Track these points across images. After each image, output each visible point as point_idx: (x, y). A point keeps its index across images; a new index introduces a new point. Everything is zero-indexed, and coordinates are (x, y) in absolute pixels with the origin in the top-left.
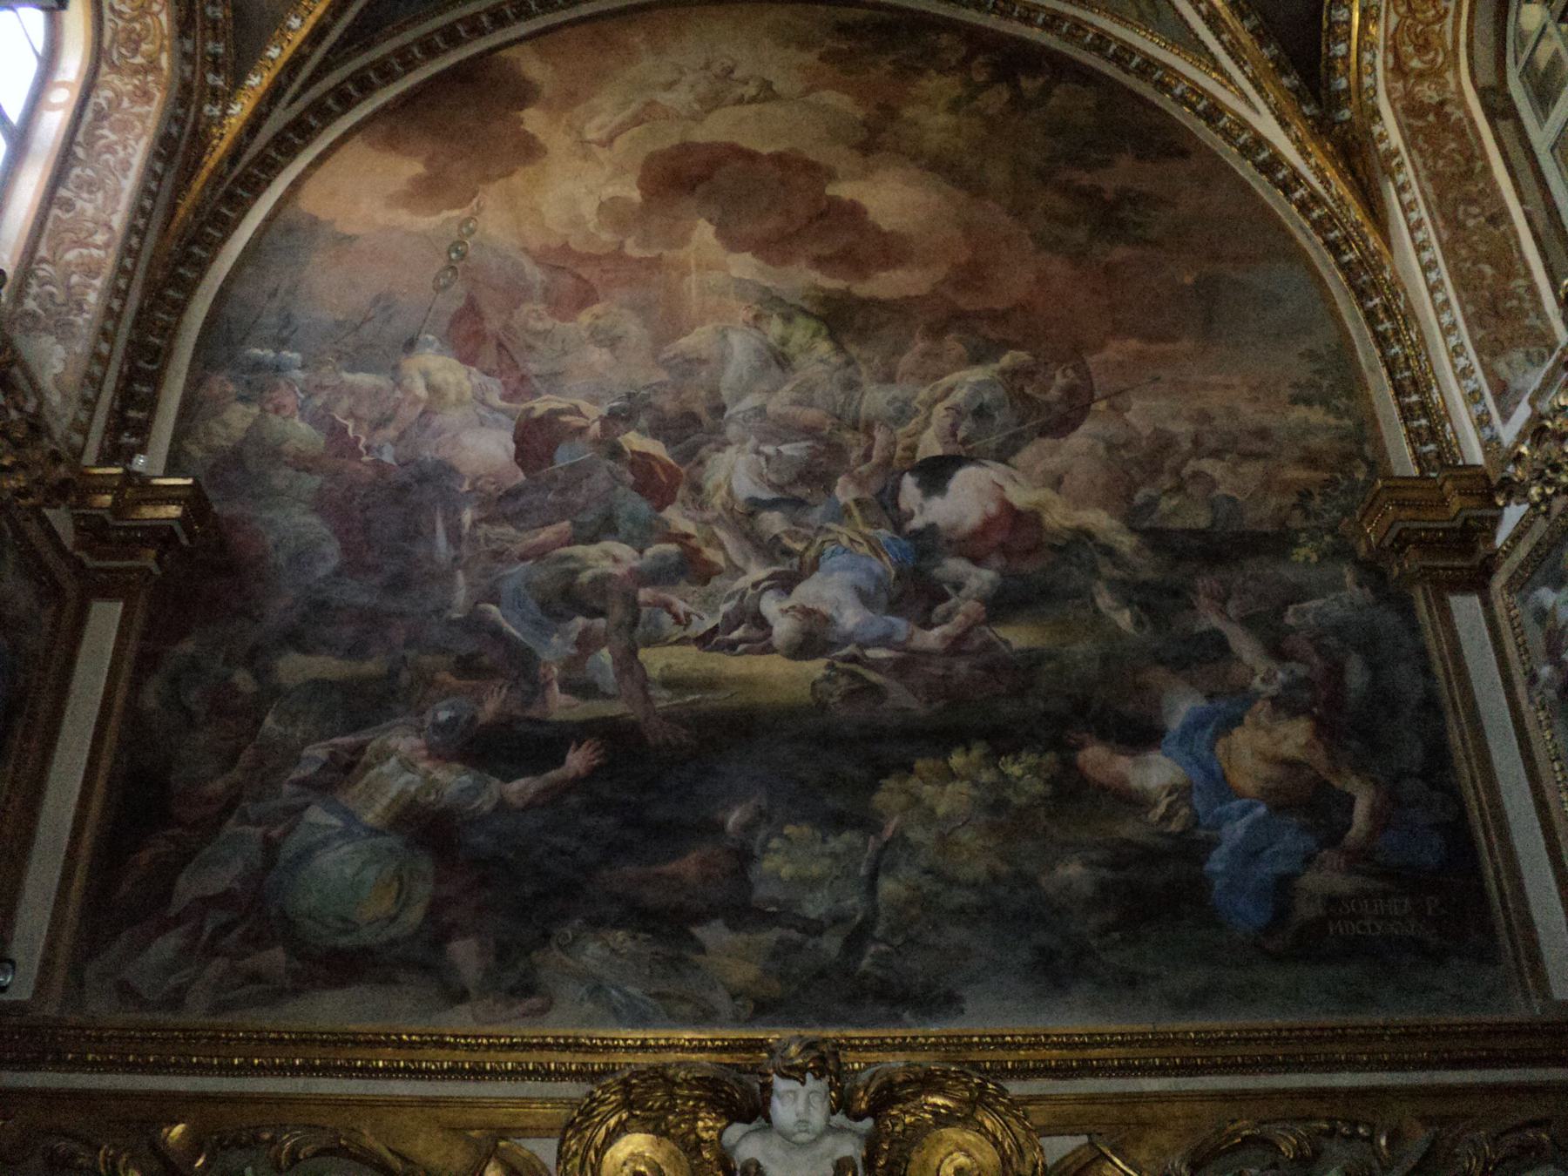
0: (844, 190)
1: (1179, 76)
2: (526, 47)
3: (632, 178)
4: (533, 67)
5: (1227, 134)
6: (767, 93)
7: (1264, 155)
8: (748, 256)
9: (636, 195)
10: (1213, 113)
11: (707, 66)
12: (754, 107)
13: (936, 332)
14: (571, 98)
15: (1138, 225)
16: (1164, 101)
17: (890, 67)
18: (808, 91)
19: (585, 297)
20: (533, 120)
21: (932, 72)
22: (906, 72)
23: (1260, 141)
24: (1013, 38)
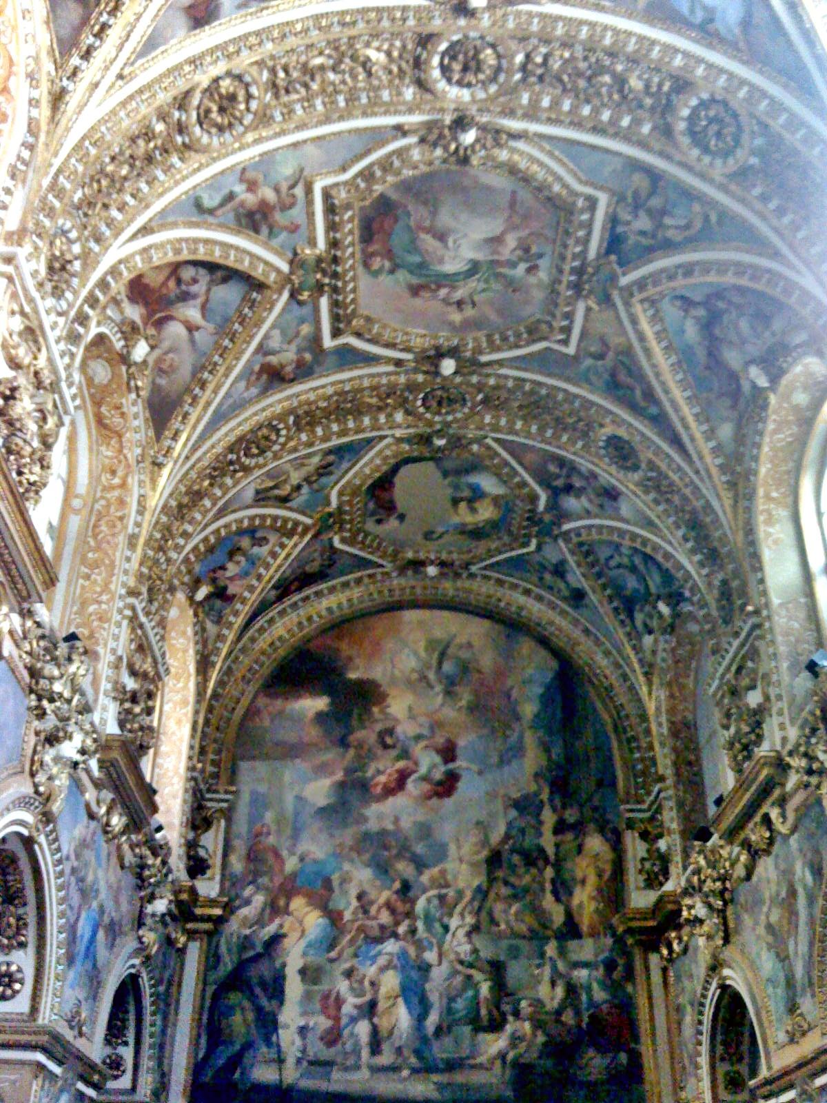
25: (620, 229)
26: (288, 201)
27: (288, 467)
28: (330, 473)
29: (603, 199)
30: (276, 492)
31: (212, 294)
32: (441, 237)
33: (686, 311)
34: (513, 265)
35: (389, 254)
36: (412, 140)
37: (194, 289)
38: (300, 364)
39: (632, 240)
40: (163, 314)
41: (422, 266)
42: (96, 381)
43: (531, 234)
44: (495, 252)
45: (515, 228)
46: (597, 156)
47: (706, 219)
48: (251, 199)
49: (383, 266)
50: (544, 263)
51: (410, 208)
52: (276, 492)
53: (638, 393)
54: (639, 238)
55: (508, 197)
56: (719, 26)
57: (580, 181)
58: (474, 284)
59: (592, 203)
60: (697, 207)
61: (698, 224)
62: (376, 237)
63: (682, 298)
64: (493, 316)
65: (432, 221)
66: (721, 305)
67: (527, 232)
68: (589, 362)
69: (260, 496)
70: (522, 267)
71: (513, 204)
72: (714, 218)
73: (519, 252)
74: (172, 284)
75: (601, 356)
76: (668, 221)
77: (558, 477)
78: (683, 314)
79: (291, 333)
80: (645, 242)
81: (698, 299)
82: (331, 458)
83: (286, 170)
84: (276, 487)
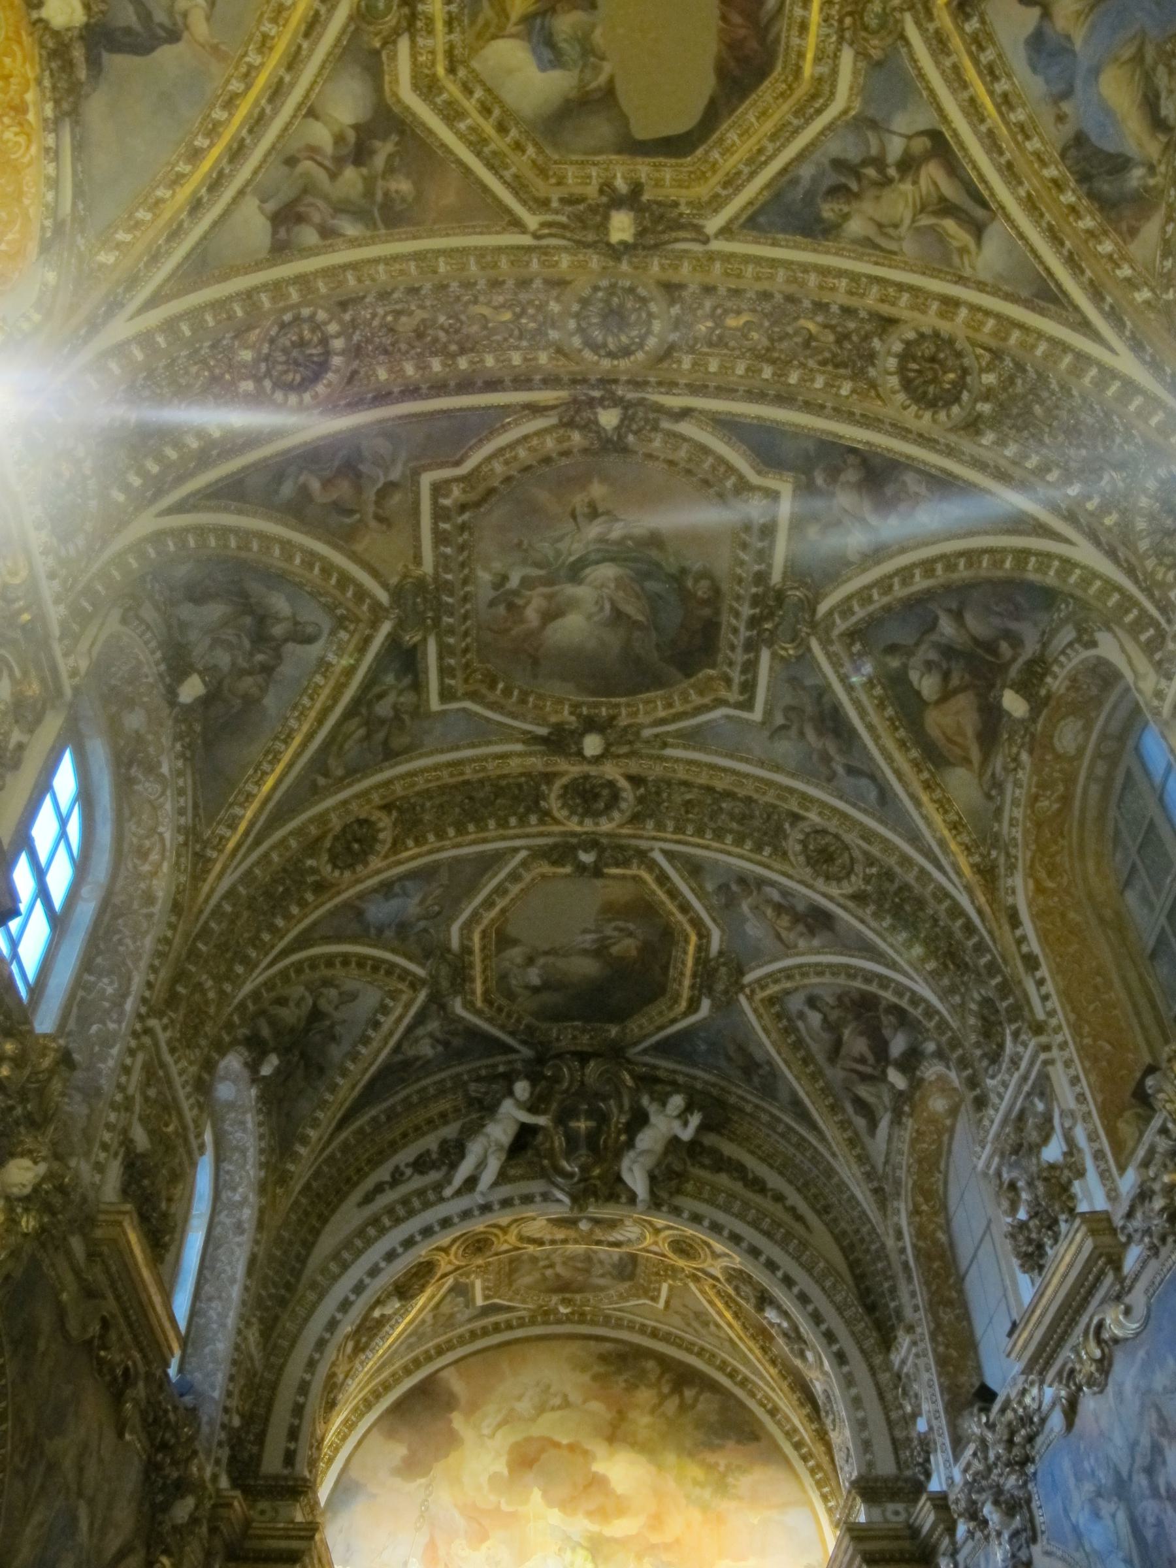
0: (599, 1467)
1: (760, 1388)
2: (452, 1369)
3: (503, 1460)
4: (456, 1383)
5: (779, 1423)
6: (566, 1404)
7: (796, 1439)
8: (556, 1510)
9: (505, 1472)
10: (773, 1412)
11: (538, 1384)
12: (558, 1414)
13: (639, 1557)
14: (473, 1407)
15: (735, 1486)
16: (751, 1404)
17: (623, 1385)
18: (585, 1402)
19: (483, 1537)
20: (457, 1420)
21: (643, 1388)
22: (632, 1387)
23: (795, 1430)
24: (680, 1363)
25: (407, 681)
27: (909, 247)
28: (839, 164)
30: (949, 189)
32: (618, 616)
33: (296, 623)
34: (526, 583)
35: (685, 596)
36: (647, 733)
38: (834, 474)
39: (390, 679)
40: (980, 651)
42: (1080, 724)
43: (508, 630)
44: (550, 597)
47: (326, 775)
48: (832, 750)
52: (949, 189)
53: (315, 485)
57: (464, 710)
58: (575, 546)
60: (340, 772)
61: (332, 762)
63: (310, 640)
64: (542, 496)
66: (260, 657)
67: (513, 633)
68: (395, 475)
69: (979, 213)
70: (514, 582)
72: (321, 781)
73: (520, 602)
74: (955, 681)
76: (362, 732)
77: (390, 170)
80: (377, 690)
81: (290, 646)
82: (828, 210)
83: (784, 747)
84: (946, 208)
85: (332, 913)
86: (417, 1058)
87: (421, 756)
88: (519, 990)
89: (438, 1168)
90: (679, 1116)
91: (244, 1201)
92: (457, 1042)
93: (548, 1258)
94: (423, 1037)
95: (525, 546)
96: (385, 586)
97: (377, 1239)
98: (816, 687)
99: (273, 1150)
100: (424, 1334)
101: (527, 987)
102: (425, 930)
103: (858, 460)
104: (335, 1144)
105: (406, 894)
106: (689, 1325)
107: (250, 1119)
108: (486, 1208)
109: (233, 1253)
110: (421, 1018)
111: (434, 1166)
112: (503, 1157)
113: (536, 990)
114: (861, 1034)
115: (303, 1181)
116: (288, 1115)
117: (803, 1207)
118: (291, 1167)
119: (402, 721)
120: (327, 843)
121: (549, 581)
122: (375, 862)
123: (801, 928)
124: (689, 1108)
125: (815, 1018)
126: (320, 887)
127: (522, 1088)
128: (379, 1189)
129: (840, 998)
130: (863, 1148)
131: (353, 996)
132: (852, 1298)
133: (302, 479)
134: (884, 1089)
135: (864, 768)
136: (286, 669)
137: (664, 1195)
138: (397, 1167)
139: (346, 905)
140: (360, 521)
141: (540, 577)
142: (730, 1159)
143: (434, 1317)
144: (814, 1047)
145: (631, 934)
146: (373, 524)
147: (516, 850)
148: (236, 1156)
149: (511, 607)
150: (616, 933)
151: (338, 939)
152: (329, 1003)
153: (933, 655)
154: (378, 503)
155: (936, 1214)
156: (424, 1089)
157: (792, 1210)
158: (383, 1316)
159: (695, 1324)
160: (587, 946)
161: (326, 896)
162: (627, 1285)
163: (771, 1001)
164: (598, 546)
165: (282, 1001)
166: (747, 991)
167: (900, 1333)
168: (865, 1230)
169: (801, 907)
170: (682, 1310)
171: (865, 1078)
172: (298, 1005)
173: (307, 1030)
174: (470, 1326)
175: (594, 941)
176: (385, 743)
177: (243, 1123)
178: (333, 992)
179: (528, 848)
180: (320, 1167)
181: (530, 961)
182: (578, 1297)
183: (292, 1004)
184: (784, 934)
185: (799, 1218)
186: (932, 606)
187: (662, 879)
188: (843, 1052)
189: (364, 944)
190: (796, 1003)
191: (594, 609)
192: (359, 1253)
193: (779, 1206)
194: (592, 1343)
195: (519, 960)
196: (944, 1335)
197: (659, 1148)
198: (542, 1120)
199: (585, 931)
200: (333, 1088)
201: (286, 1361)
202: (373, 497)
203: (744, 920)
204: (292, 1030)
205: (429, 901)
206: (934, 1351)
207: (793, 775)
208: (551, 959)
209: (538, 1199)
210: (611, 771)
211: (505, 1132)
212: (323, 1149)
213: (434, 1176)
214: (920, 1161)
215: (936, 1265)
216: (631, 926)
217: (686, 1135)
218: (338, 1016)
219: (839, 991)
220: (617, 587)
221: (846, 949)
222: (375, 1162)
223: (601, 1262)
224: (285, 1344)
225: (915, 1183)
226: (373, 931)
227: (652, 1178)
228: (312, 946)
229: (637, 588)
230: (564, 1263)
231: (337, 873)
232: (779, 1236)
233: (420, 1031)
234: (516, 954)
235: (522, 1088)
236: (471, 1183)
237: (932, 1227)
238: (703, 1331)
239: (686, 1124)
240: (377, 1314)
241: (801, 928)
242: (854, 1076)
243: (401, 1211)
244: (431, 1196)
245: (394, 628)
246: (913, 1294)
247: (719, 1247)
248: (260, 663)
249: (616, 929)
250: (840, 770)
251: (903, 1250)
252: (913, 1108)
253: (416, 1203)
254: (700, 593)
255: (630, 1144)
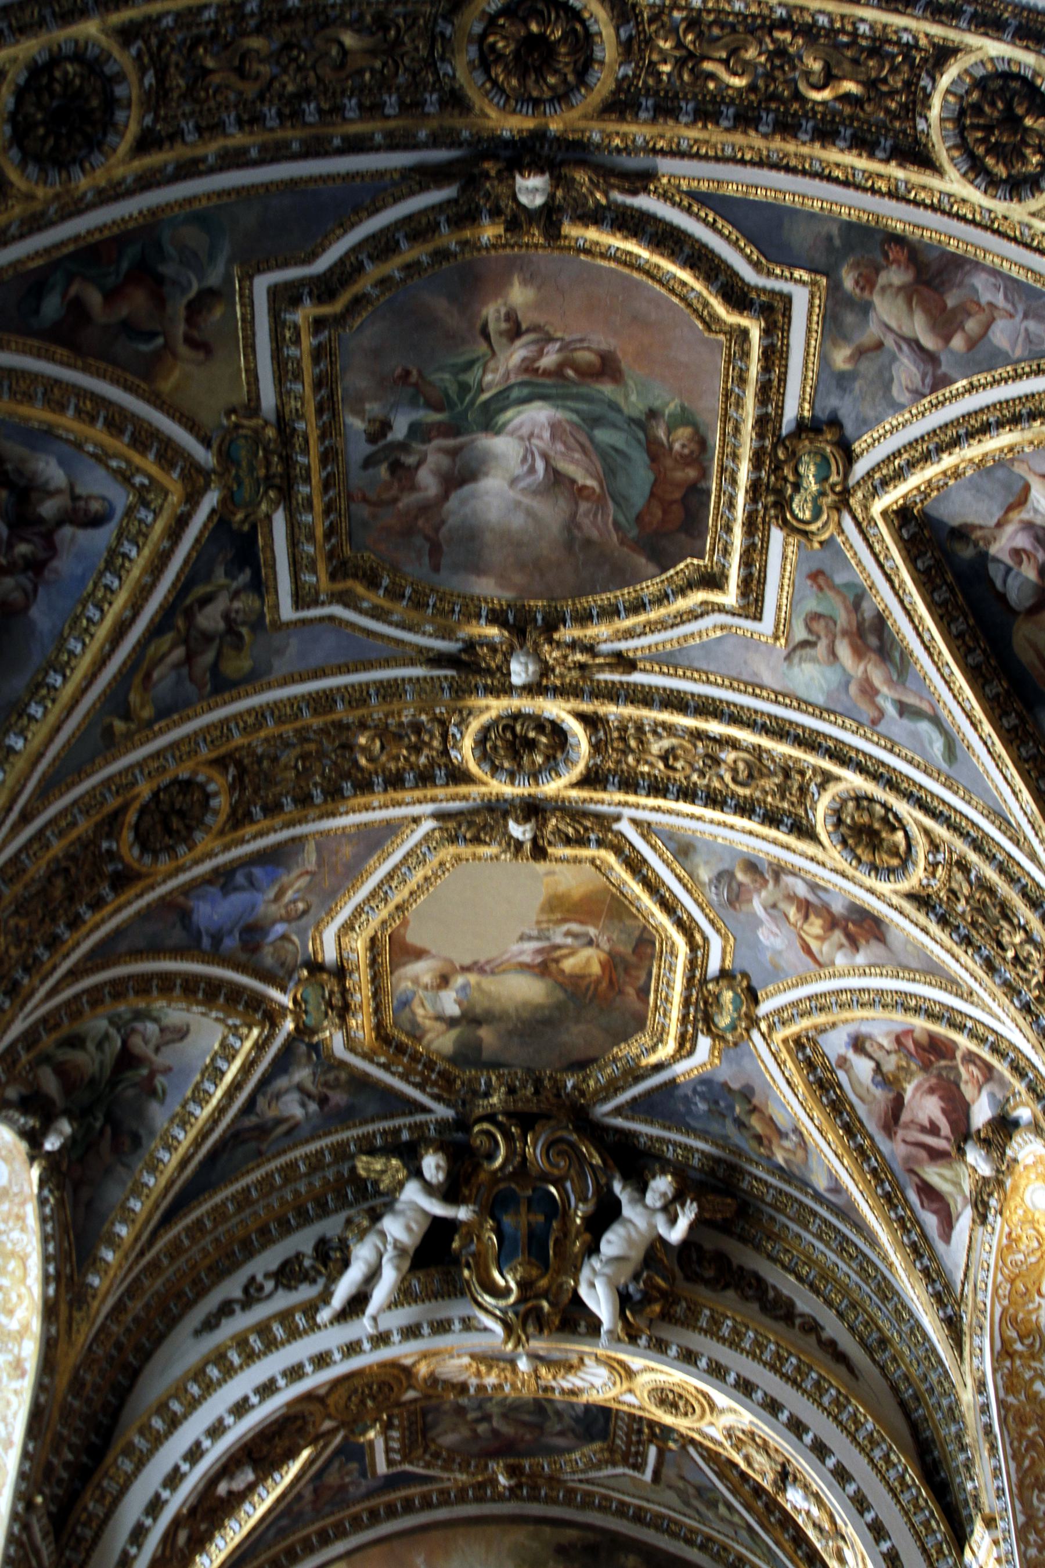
25: (245, 577)
26: (819, 627)
29: (287, 612)
31: (998, 515)
32: (556, 479)
33: (75, 498)
34: (417, 431)
35: (655, 452)
37: (1023, 541)
39: (220, 577)
41: (594, 421)
43: (395, 500)
44: (453, 453)
45: (426, 508)
46: (315, 659)
47: (127, 716)
48: (877, 677)
49: (669, 432)
50: (359, 449)
51: (615, 537)
53: (94, 298)
54: (209, 589)
55: (444, 561)
56: (213, 890)
57: (331, 618)
58: (489, 378)
59: (300, 600)
60: (147, 713)
61: (134, 698)
62: (677, 495)
63: (96, 521)
65: (574, 515)
66: (23, 548)
68: (214, 278)
70: (399, 431)
71: (436, 550)
72: (119, 726)
73: (410, 460)
75: (196, 309)
76: (179, 653)
78: (79, 490)
79: (868, 367)
80: (200, 591)
81: (67, 531)
85: (143, 916)
86: (279, 1121)
87: (270, 687)
88: (428, 1023)
89: (314, 1281)
90: (665, 1209)
91: (26, 1327)
92: (339, 1098)
93: (480, 1407)
94: (287, 1091)
95: (414, 377)
96: (206, 442)
97: (220, 1383)
98: (850, 586)
99: (68, 1257)
100: (301, 1514)
101: (439, 1018)
102: (284, 937)
103: (903, 256)
104: (160, 1245)
105: (252, 883)
106: (687, 1504)
107: (31, 1212)
108: (381, 1339)
109: (8, 1404)
110: (283, 1063)
111: (308, 1278)
112: (406, 1264)
113: (452, 1022)
114: (931, 1091)
115: (110, 1302)
116: (89, 1204)
117: (848, 1344)
118: (95, 1281)
119: (240, 636)
120: (131, 817)
121: (452, 429)
122: (204, 842)
123: (838, 936)
124: (679, 1197)
125: (863, 1067)
126: (122, 880)
127: (432, 1165)
128: (226, 1309)
129: (898, 1040)
130: (934, 1257)
131: (182, 1033)
132: (912, 1476)
133: (73, 290)
134: (963, 1171)
135: (925, 706)
136: (64, 565)
137: (640, 1322)
138: (253, 1279)
139: (165, 904)
140: (166, 346)
141: (439, 424)
142: (741, 1268)
143: (315, 1491)
144: (862, 1110)
145: (590, 943)
146: (183, 350)
147: (416, 820)
148: (12, 1265)
149: (396, 467)
150: (569, 941)
151: (156, 951)
152: (146, 1042)
153: (1023, 541)
154: (190, 321)
155: (1033, 1356)
156: (293, 1165)
157: (831, 1348)
158: (230, 1493)
159: (696, 1503)
160: (527, 958)
161: (131, 892)
162: (597, 1446)
163: (798, 1043)
164: (526, 377)
165: (76, 1042)
166: (763, 1026)
167: (979, 1527)
168: (933, 1377)
169: (838, 907)
170: (681, 1484)
171: (936, 1155)
172: (100, 1046)
173: (114, 1082)
174: (367, 1504)
175: (539, 951)
176: (215, 668)
177: (20, 1218)
178: (151, 1028)
179: (438, 816)
180: (137, 1279)
181: (444, 981)
182: (526, 1464)
183: (91, 1047)
184: (814, 945)
185: (841, 1358)
186: (1020, 469)
187: (636, 865)
188: (905, 1117)
189: (192, 960)
190: (835, 1045)
191: (520, 470)
192: (194, 1404)
193: (812, 1339)
194: (547, 1530)
195: (426, 979)
196: (1038, 1532)
197: (637, 1255)
198: (463, 1213)
199: (523, 938)
200: (153, 1168)
201: (88, 1556)
202: (182, 312)
203: (758, 923)
204: (92, 1081)
205: (289, 895)
206: (1023, 1555)
207: (822, 712)
208: (473, 978)
209: (457, 1326)
210: (555, 709)
211: (409, 1229)
212: (142, 1254)
213: (306, 1292)
214: (1012, 1282)
215: (1031, 1431)
216: (592, 931)
217: (676, 1234)
218: (160, 1060)
219: (899, 1029)
220: (553, 436)
221: (902, 969)
222: (220, 1272)
223: (559, 1414)
224: (89, 1533)
225: (1005, 1310)
226: (206, 942)
227: (624, 1300)
228: (116, 963)
229: (583, 439)
230: (505, 1416)
231: (148, 859)
232: (808, 1385)
233: (282, 1083)
234: (423, 970)
235: (432, 1165)
236: (358, 1303)
237: (1028, 1375)
238: (710, 1515)
239: (673, 1221)
240: (222, 1488)
241: (838, 936)
242: (923, 1154)
243: (256, 1343)
244: (300, 1320)
245: (223, 502)
246: (996, 1473)
247: (721, 1399)
248: (24, 557)
249: (568, 934)
250: (891, 710)
251: (985, 1409)
252: (1004, 1201)
253: (278, 1331)
254: (677, 446)
255: (593, 1249)
